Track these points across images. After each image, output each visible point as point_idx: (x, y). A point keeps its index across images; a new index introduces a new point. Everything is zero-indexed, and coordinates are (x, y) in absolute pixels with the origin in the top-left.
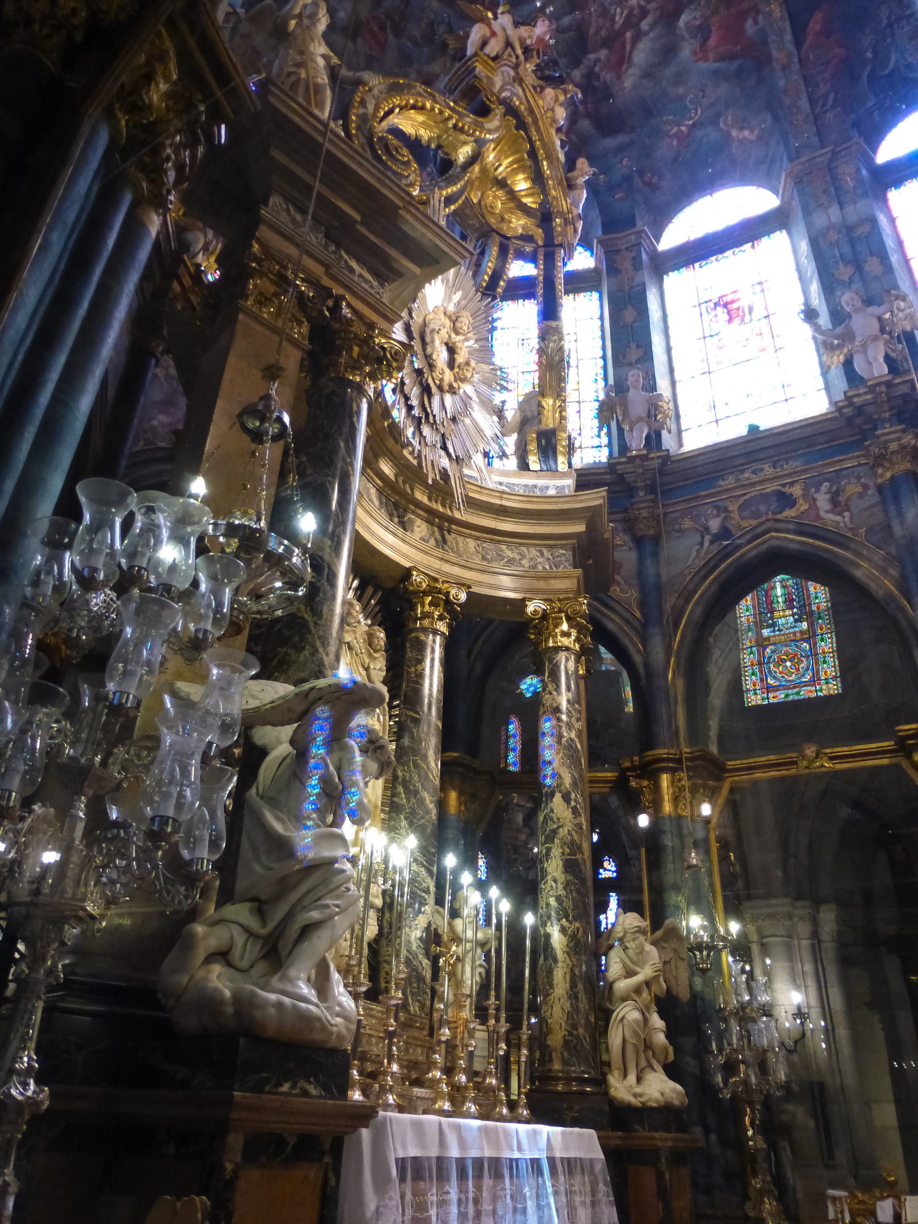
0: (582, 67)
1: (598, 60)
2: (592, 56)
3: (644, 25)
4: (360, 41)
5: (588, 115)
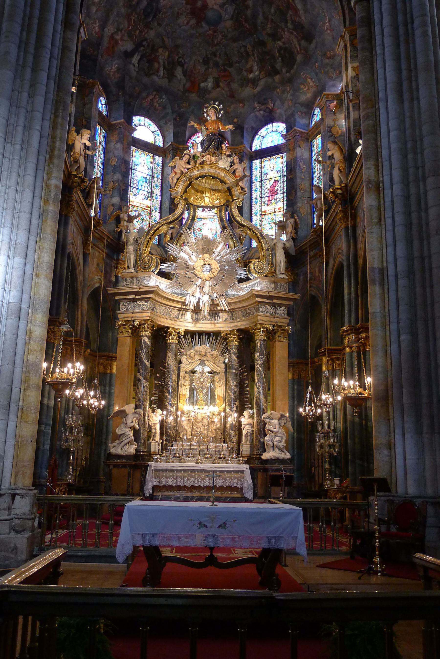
0: (289, 21)
1: (291, 15)
2: (288, 15)
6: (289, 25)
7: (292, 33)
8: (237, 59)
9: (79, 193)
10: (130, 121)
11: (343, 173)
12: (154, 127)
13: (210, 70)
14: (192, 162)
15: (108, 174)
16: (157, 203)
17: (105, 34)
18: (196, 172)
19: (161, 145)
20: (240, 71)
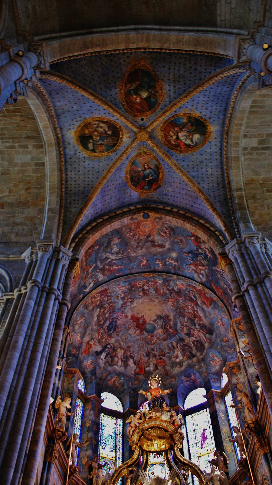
2: (196, 321)
3: (196, 309)
4: (159, 367)
5: (207, 333)
6: (197, 327)
7: (199, 331)
8: (167, 351)
9: (61, 444)
10: (100, 397)
11: (252, 412)
12: (116, 399)
13: (151, 359)
14: (143, 418)
15: (84, 433)
16: (120, 454)
17: (84, 341)
18: (146, 425)
19: (122, 411)
20: (170, 358)
